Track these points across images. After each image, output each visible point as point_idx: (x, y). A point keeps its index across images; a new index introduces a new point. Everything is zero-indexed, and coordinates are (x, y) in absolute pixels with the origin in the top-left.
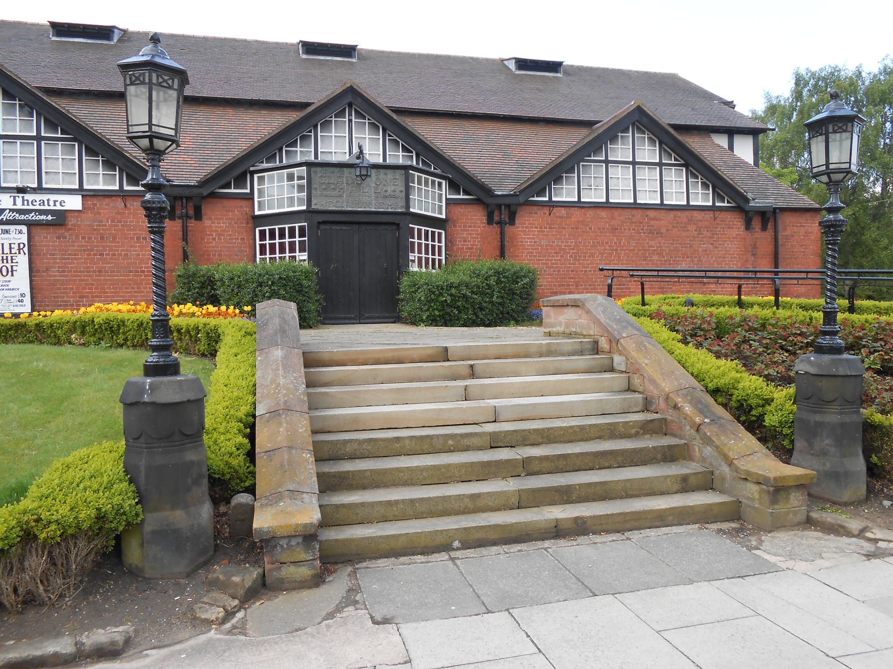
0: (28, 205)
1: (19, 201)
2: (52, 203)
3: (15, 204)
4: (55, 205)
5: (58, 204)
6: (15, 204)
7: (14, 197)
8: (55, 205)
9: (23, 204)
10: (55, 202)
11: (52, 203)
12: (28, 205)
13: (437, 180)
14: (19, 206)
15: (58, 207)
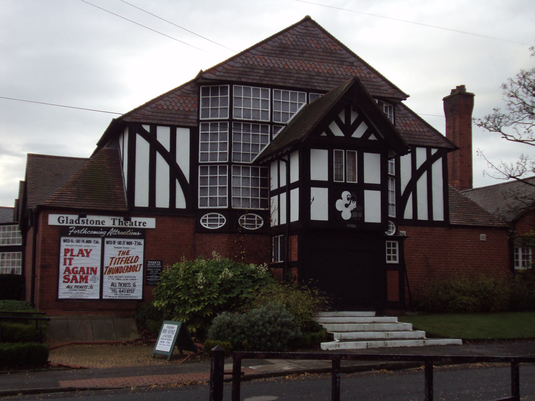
0: (122, 225)
1: (117, 222)
2: (137, 224)
3: (114, 224)
4: (139, 225)
5: (141, 224)
6: (114, 224)
7: (114, 220)
8: (139, 225)
9: (119, 224)
10: (140, 223)
11: (137, 224)
12: (122, 225)
13: (392, 242)
14: (117, 225)
15: (142, 226)
